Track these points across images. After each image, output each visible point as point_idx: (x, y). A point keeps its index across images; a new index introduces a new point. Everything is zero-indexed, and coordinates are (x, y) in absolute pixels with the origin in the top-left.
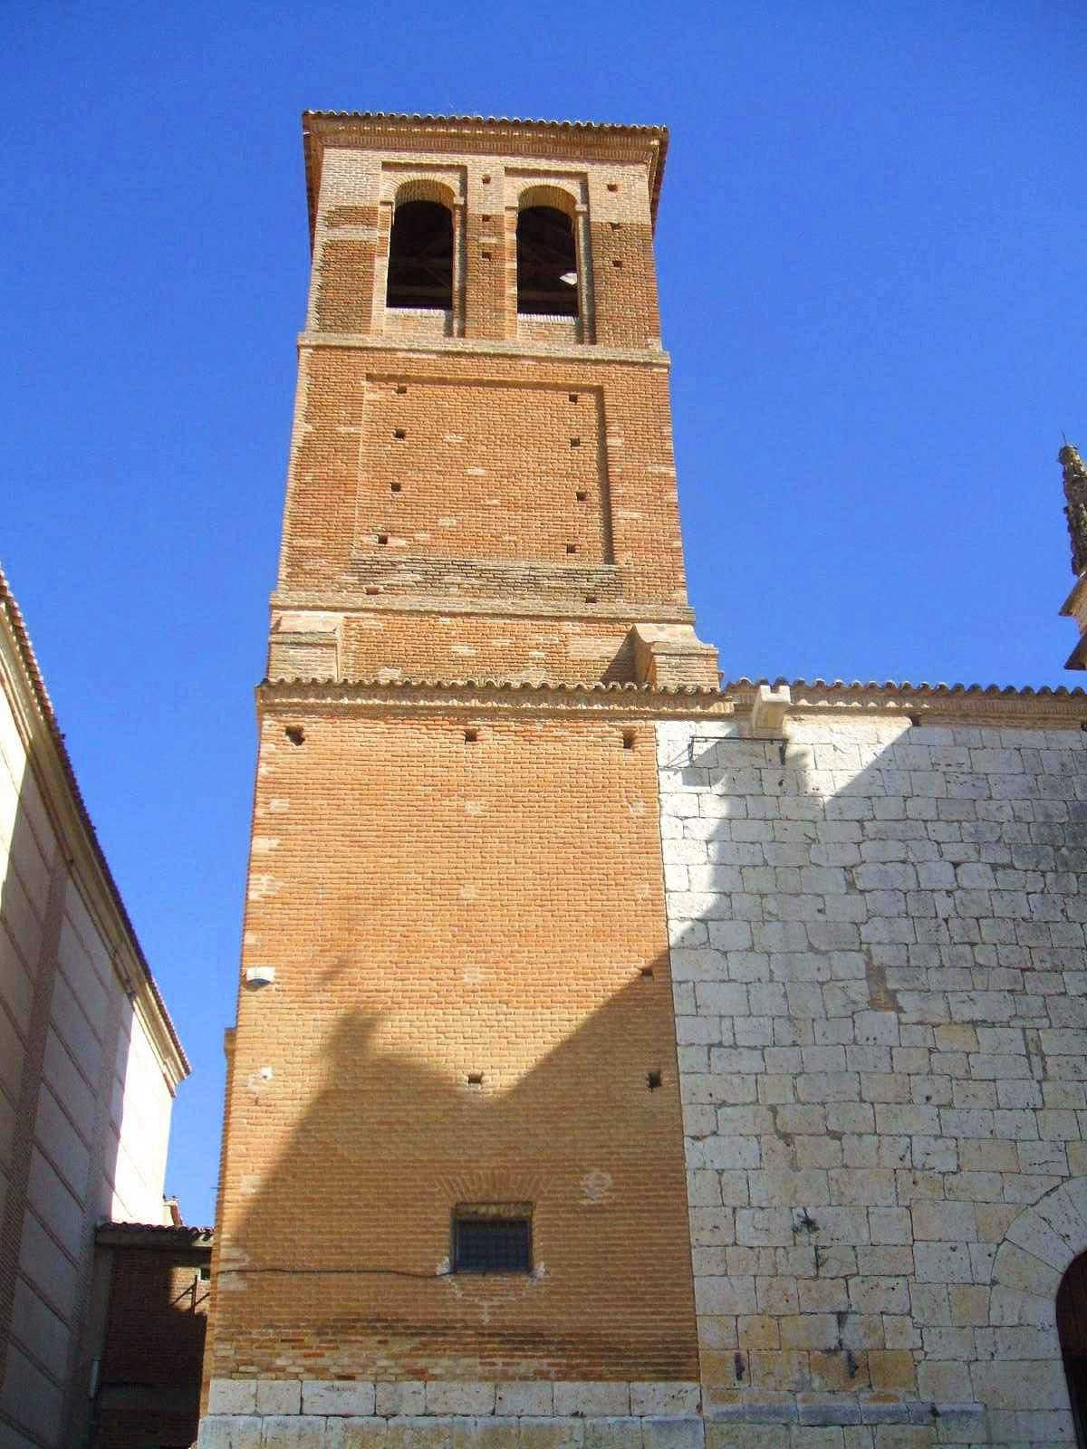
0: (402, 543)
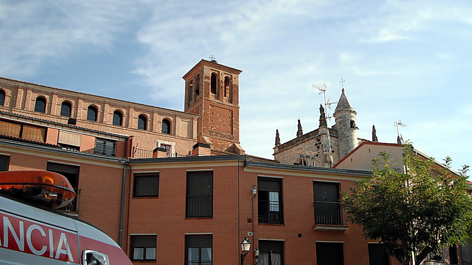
0: (213, 129)
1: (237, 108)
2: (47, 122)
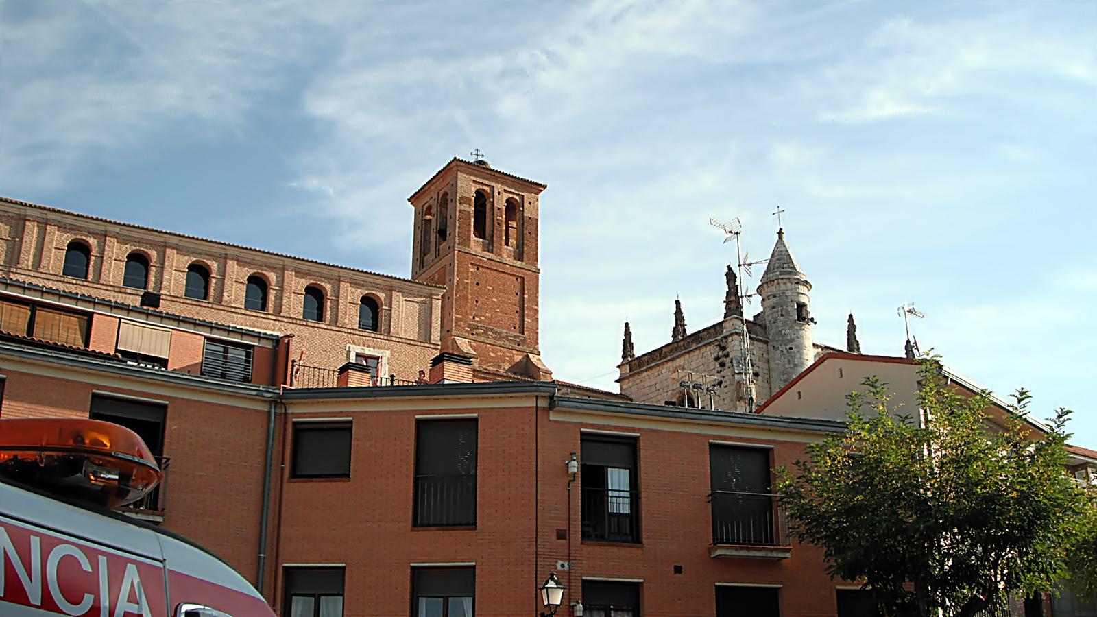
0: (478, 319)
1: (535, 272)
2: (93, 300)
